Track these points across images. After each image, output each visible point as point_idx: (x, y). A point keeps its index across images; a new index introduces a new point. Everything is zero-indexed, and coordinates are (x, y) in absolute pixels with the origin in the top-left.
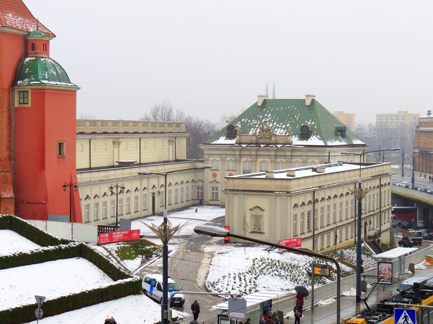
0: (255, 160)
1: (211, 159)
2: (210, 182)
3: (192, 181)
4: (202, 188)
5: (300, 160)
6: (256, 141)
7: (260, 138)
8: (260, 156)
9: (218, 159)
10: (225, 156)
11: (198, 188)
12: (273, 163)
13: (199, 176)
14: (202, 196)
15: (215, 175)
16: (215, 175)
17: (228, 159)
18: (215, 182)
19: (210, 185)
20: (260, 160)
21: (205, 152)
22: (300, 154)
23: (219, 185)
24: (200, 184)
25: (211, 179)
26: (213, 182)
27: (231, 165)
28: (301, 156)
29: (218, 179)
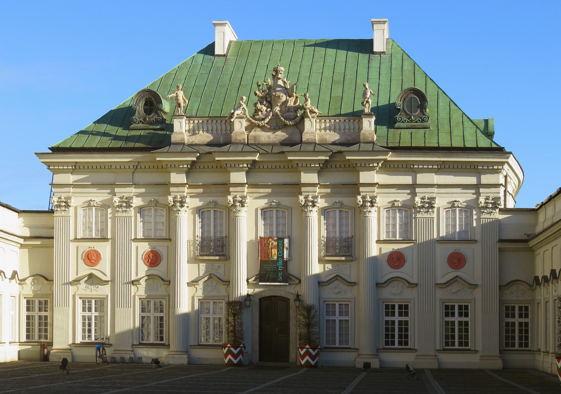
3: (13, 277)
15: (92, 258)
16: (92, 258)
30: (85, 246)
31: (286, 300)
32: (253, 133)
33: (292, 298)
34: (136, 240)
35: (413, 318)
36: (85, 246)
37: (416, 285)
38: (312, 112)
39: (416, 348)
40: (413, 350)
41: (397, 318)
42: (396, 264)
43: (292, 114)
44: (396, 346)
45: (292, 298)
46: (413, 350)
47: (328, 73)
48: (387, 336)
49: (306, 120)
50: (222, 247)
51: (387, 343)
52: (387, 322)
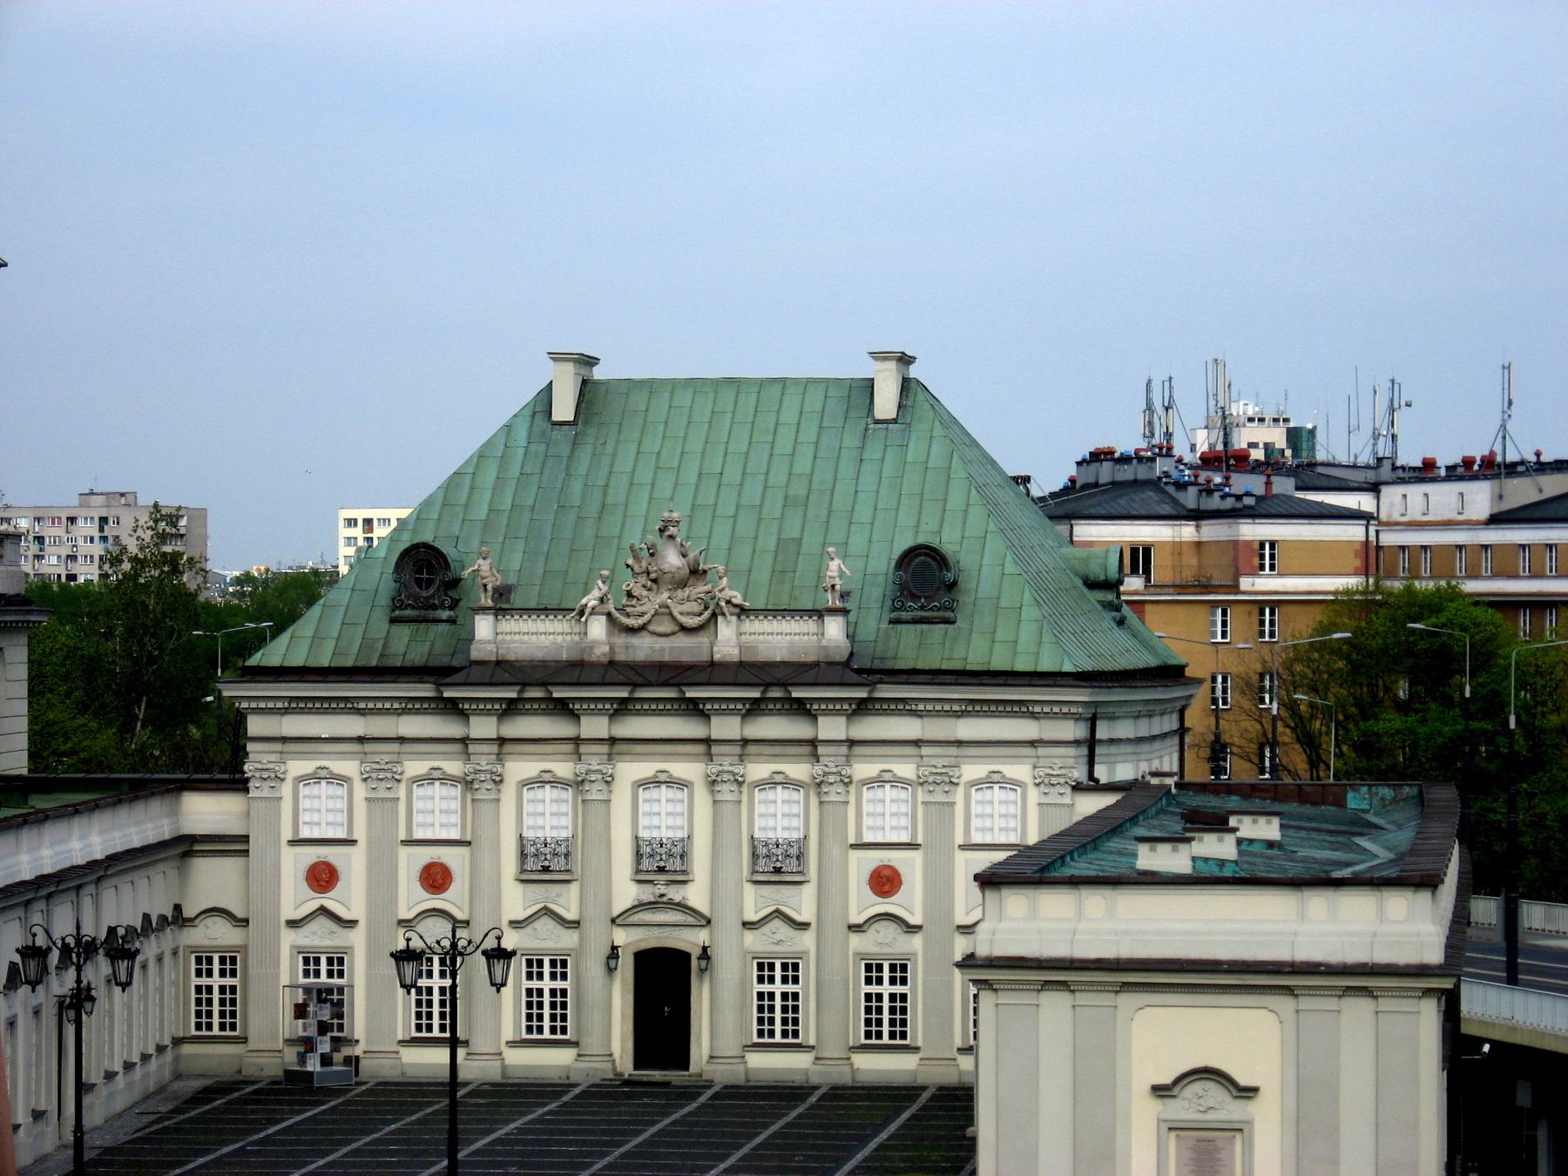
0: (608, 769)
1: (298, 767)
2: (293, 924)
4: (230, 964)
5: (906, 770)
6: (612, 648)
7: (632, 631)
8: (639, 748)
9: (348, 767)
10: (395, 747)
11: (203, 963)
12: (726, 792)
13: (212, 881)
14: (229, 1016)
15: (322, 877)
16: (322, 877)
17: (415, 767)
18: (323, 921)
19: (289, 938)
20: (630, 770)
21: (255, 726)
22: (907, 728)
23: (356, 939)
24: (218, 934)
25: (294, 898)
26: (538, 925)
27: (437, 812)
28: (917, 743)
29: (350, 898)
30: (313, 854)
31: (687, 956)
32: (621, 640)
33: (695, 953)
34: (406, 843)
35: (917, 989)
36: (313, 854)
37: (919, 927)
38: (728, 602)
39: (920, 1044)
40: (916, 1049)
41: (886, 989)
42: (886, 888)
43: (696, 607)
44: (886, 1040)
45: (695, 953)
46: (916, 1049)
47: (778, 477)
48: (868, 1022)
49: (720, 618)
50: (567, 855)
51: (868, 1035)
52: (868, 997)
